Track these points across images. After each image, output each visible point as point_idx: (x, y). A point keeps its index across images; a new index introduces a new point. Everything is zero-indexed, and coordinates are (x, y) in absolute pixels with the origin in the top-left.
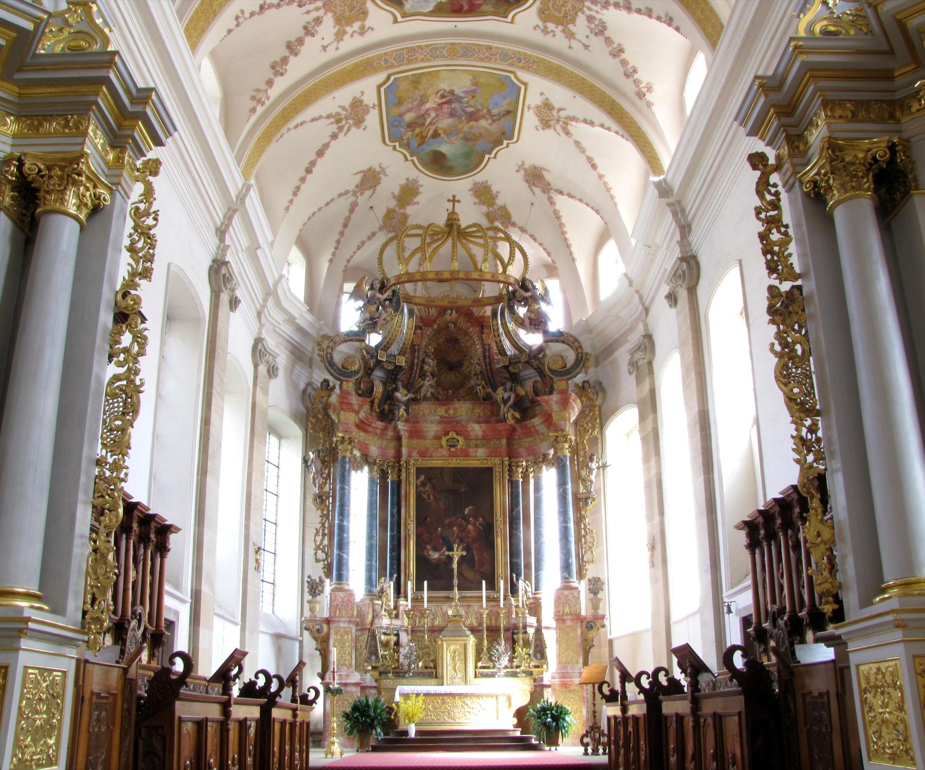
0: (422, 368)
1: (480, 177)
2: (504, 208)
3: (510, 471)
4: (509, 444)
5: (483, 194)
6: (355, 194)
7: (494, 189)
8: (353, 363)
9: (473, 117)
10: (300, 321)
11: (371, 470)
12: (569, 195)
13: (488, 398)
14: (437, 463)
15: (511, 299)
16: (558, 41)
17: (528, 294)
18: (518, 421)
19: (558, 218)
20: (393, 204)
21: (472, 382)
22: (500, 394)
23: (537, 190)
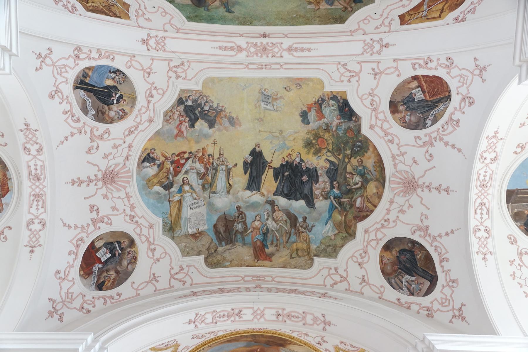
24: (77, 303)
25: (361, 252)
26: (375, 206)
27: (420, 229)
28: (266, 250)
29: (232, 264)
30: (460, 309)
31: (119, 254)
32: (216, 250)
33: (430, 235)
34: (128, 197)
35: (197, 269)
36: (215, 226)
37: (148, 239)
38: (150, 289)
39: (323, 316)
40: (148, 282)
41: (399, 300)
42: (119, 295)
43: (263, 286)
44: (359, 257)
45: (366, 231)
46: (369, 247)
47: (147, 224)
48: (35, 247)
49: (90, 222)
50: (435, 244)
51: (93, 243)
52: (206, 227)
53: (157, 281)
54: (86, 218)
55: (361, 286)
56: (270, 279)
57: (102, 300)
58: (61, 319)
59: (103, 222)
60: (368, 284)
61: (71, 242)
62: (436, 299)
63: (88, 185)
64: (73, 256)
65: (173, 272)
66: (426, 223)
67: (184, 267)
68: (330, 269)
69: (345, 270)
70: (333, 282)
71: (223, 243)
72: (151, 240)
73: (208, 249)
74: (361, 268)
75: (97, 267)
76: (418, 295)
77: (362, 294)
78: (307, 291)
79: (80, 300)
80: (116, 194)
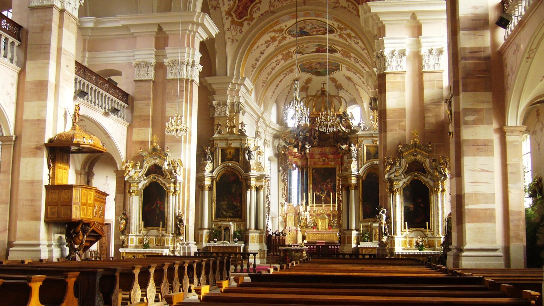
0: (314, 135)
2: (340, 84)
4: (341, 160)
5: (333, 80)
6: (291, 85)
7: (337, 79)
8: (292, 141)
11: (298, 169)
12: (359, 86)
13: (335, 146)
14: (319, 166)
15: (341, 118)
16: (347, 59)
17: (346, 118)
19: (357, 90)
21: (331, 141)
23: (350, 82)
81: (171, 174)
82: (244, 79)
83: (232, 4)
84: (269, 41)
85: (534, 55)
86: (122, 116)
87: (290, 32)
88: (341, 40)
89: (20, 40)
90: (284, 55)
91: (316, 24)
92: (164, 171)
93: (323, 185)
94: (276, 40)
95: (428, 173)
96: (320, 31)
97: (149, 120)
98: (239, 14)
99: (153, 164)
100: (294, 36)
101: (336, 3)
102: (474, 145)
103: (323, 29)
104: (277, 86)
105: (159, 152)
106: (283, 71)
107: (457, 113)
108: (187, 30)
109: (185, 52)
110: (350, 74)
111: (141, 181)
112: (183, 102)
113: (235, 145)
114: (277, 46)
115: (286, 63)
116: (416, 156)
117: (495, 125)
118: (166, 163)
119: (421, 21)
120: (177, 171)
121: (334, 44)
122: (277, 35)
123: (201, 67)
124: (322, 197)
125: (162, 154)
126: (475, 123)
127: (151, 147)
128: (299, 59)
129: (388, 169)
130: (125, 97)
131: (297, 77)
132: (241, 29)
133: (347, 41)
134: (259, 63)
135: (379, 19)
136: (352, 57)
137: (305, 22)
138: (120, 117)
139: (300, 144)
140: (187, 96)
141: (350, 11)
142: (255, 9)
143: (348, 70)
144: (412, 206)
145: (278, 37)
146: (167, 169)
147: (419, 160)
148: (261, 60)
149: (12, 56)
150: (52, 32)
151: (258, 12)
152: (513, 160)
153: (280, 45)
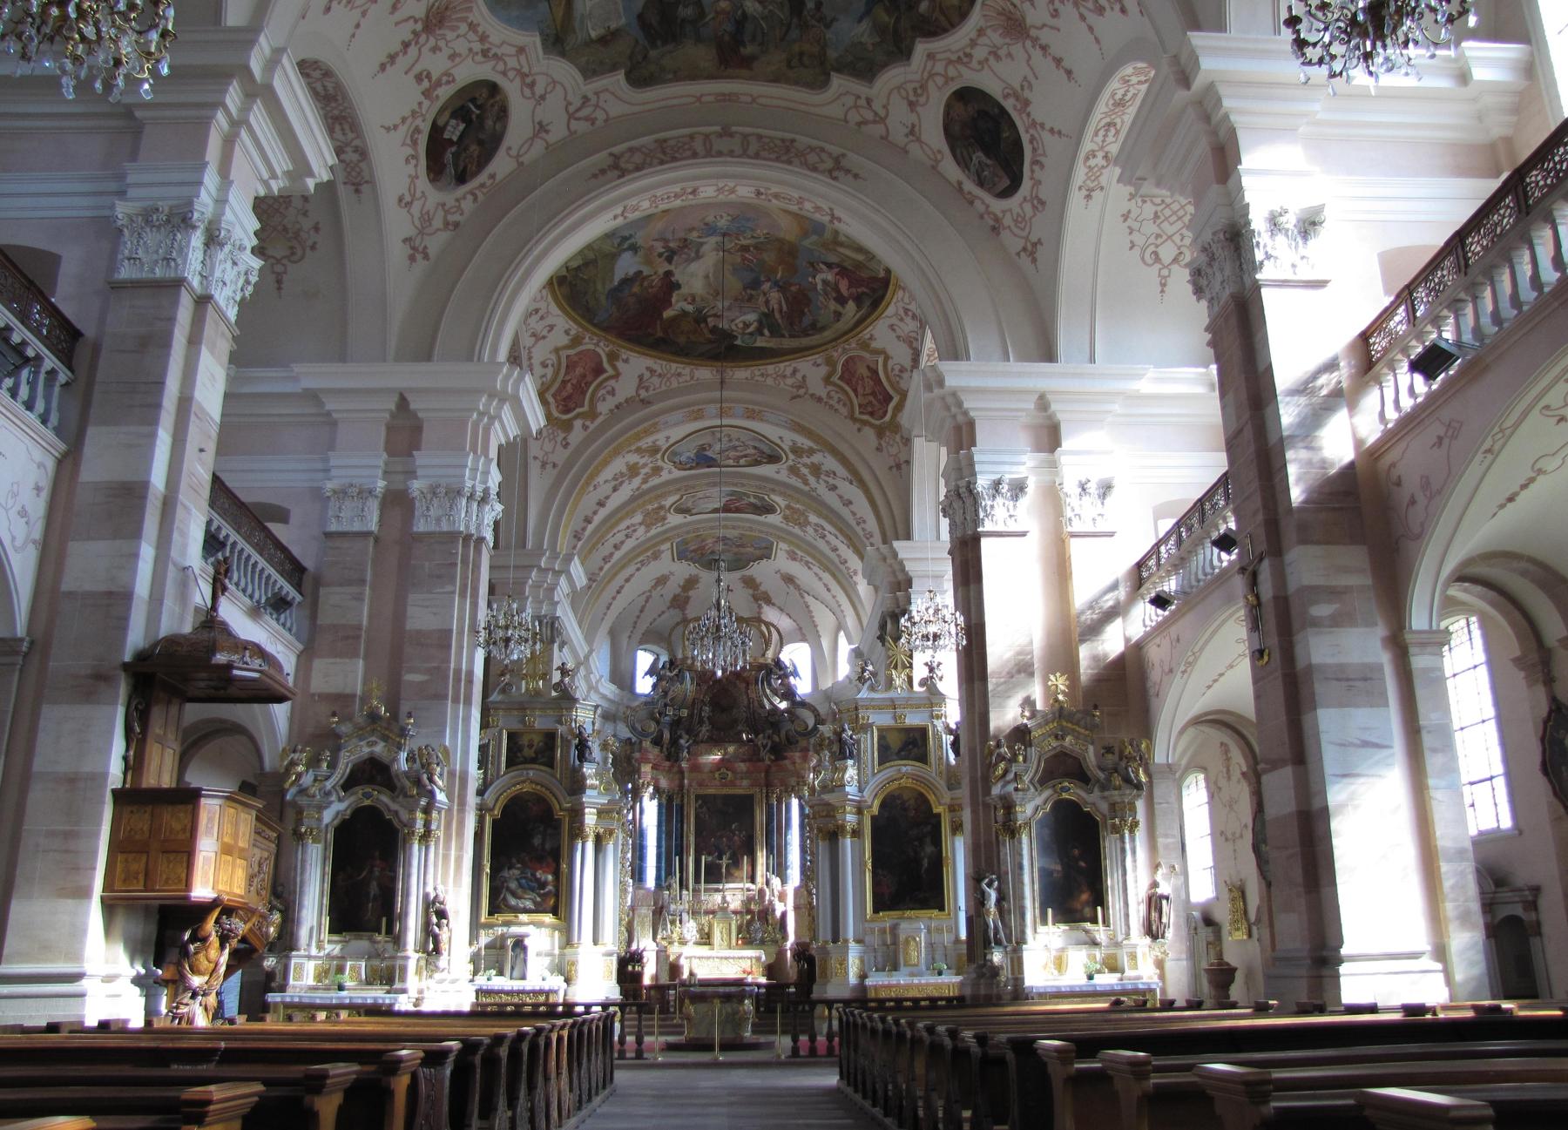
1: (746, 572)
2: (766, 593)
3: (767, 796)
5: (750, 583)
7: (758, 581)
9: (738, 546)
10: (611, 696)
11: (659, 800)
14: (711, 791)
15: (769, 672)
16: (797, 530)
18: (772, 761)
19: (808, 607)
20: (679, 590)
22: (761, 740)
23: (792, 587)
24: (438, 223)
25: (917, 85)
26: (953, 26)
27: (1017, 99)
28: (742, 49)
29: (679, 76)
30: (1034, 245)
31: (478, 116)
32: (645, 57)
33: (1029, 115)
34: (472, 27)
35: (613, 93)
36: (640, 17)
37: (519, 72)
38: (539, 146)
39: (831, 209)
40: (532, 139)
41: (960, 183)
42: (492, 176)
43: (734, 129)
44: (911, 93)
45: (931, 56)
46: (931, 84)
47: (513, 51)
48: (360, 184)
49: (422, 98)
50: (1032, 131)
51: (434, 124)
52: (623, 21)
53: (547, 132)
54: (411, 94)
55: (906, 140)
56: (749, 99)
57: (470, 197)
58: (426, 257)
59: (440, 85)
60: (919, 140)
61: (404, 144)
62: (1010, 210)
63: (405, 53)
64: (413, 162)
65: (571, 109)
66: (1027, 94)
67: (590, 95)
68: (859, 97)
69: (884, 107)
70: (858, 119)
71: (659, 43)
72: (526, 70)
73: (630, 58)
74: (912, 111)
75: (448, 157)
76: (989, 190)
77: (907, 152)
78: (812, 149)
79: (440, 213)
80: (450, 35)
81: (418, 782)
82: (568, 559)
83: (549, 376)
84: (622, 475)
85: (1503, 446)
86: (288, 625)
87: (672, 454)
88: (795, 481)
89: (70, 368)
90: (647, 515)
91: (738, 440)
92: (397, 776)
93: (721, 837)
94: (637, 474)
95: (1093, 781)
96: (745, 456)
97: (358, 637)
98: (564, 400)
99: (366, 757)
100: (680, 466)
101: (799, 387)
102: (1338, 680)
103: (753, 451)
104: (618, 592)
105: (384, 725)
106: (638, 555)
107: (1283, 604)
108: (471, 410)
109: (466, 466)
110: (795, 569)
111: (331, 802)
112: (454, 592)
113: (540, 722)
114: (638, 489)
115: (649, 535)
116: (1063, 738)
117: (1381, 631)
118: (403, 756)
119: (1060, 416)
120: (436, 778)
121: (773, 491)
122: (642, 461)
123: (499, 507)
124: (720, 867)
125: (391, 731)
126: (1336, 621)
127: (361, 710)
128: (675, 528)
129: (1000, 771)
130: (295, 570)
131: (666, 572)
132: (565, 439)
133: (806, 482)
134: (590, 528)
135: (960, 404)
136: (809, 523)
137: (713, 433)
138: (284, 625)
139: (667, 735)
140: (464, 577)
141: (831, 407)
142: (602, 392)
143: (793, 556)
144: (1059, 868)
145: (645, 465)
146: (405, 772)
147: (1072, 751)
148: (597, 520)
149: (47, 411)
150: (173, 352)
151: (609, 398)
152: (1433, 716)
153: (645, 487)
